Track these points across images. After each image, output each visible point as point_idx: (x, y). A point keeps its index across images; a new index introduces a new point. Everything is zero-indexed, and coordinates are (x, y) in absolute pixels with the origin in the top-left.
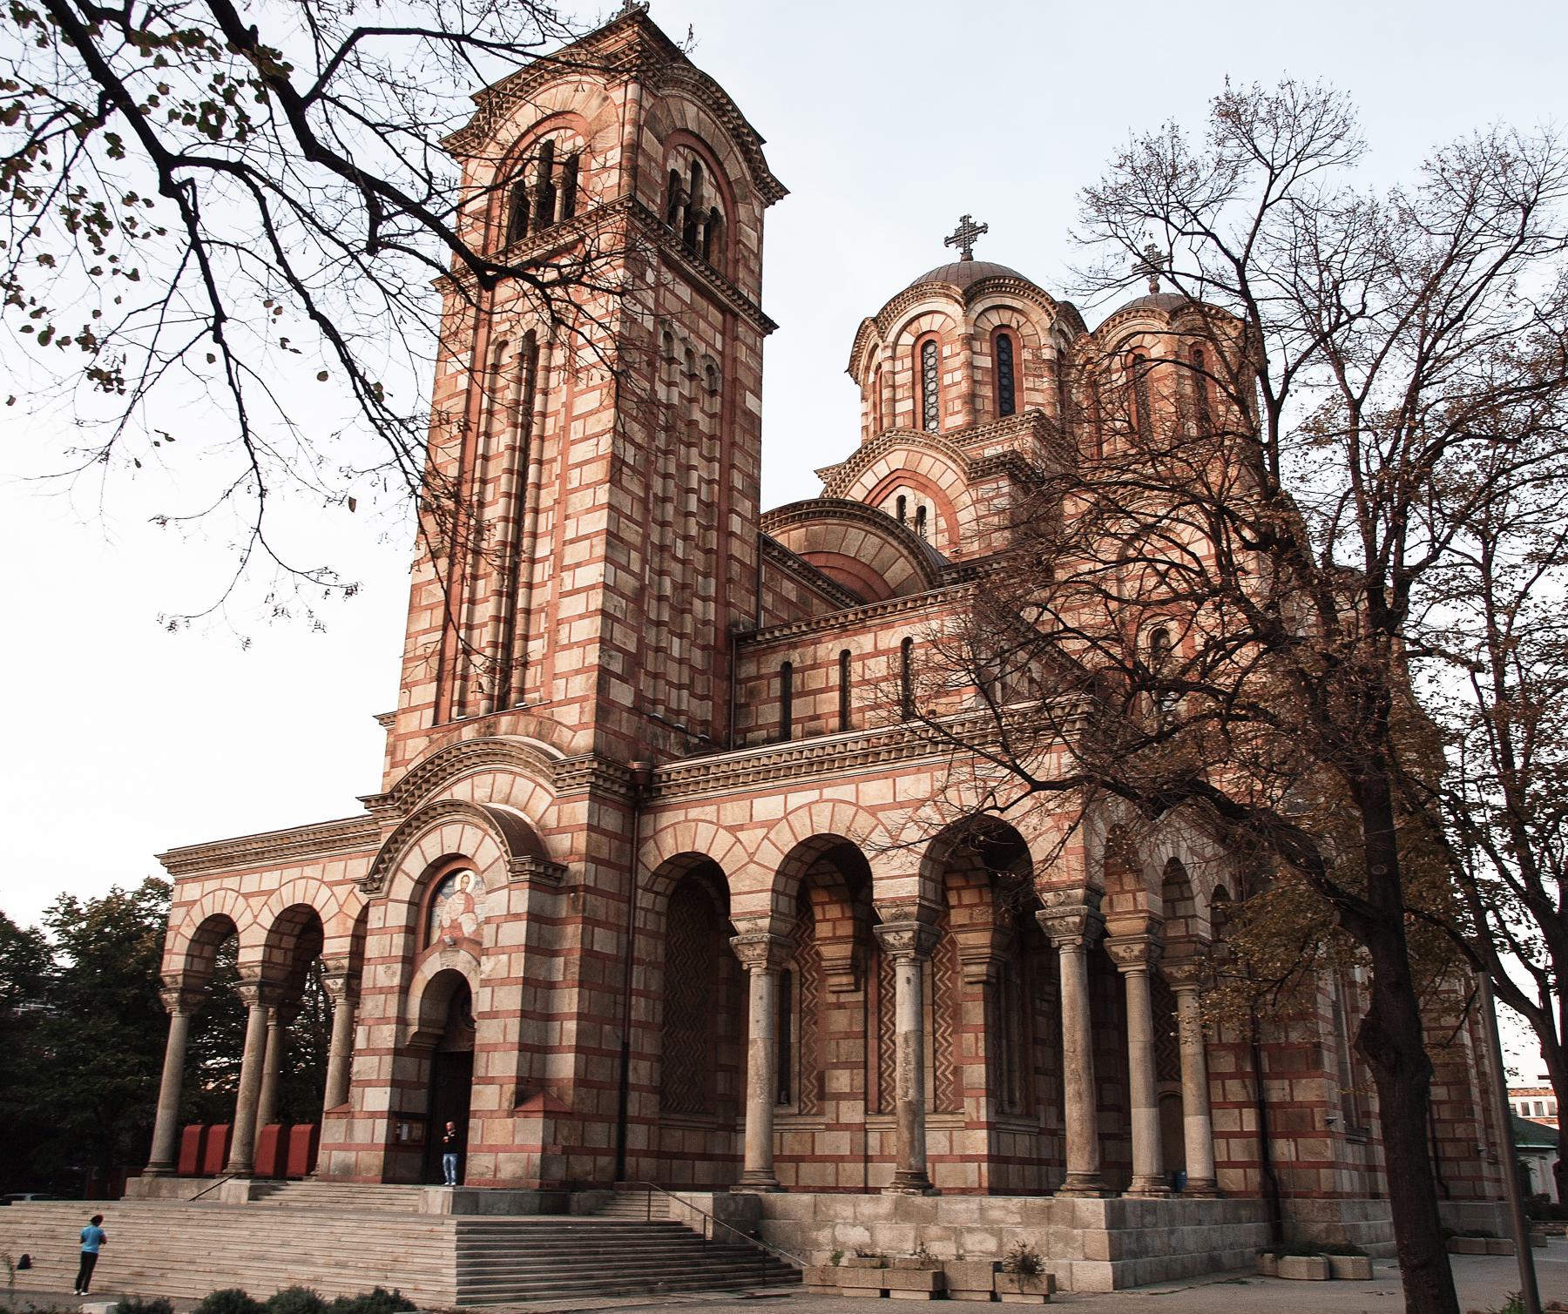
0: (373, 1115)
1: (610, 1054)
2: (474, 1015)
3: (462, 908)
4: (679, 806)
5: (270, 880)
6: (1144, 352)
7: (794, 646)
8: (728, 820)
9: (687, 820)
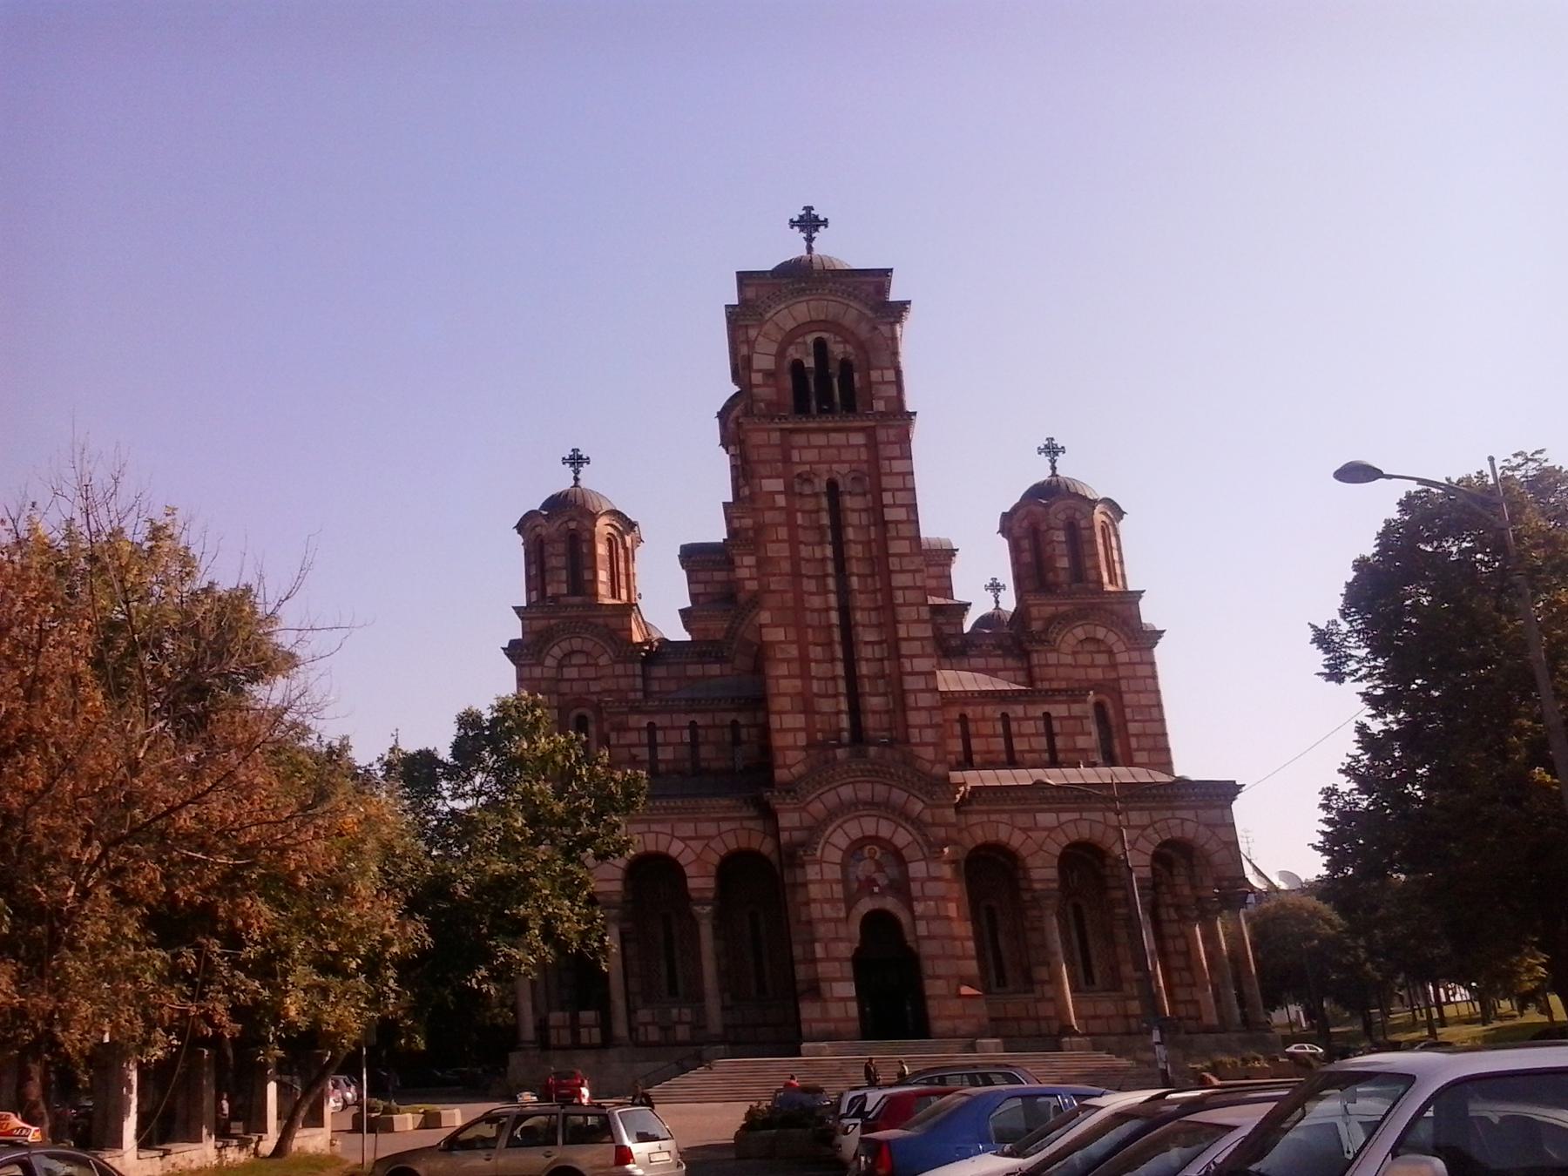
3: (873, 868)
4: (982, 812)
7: (966, 704)
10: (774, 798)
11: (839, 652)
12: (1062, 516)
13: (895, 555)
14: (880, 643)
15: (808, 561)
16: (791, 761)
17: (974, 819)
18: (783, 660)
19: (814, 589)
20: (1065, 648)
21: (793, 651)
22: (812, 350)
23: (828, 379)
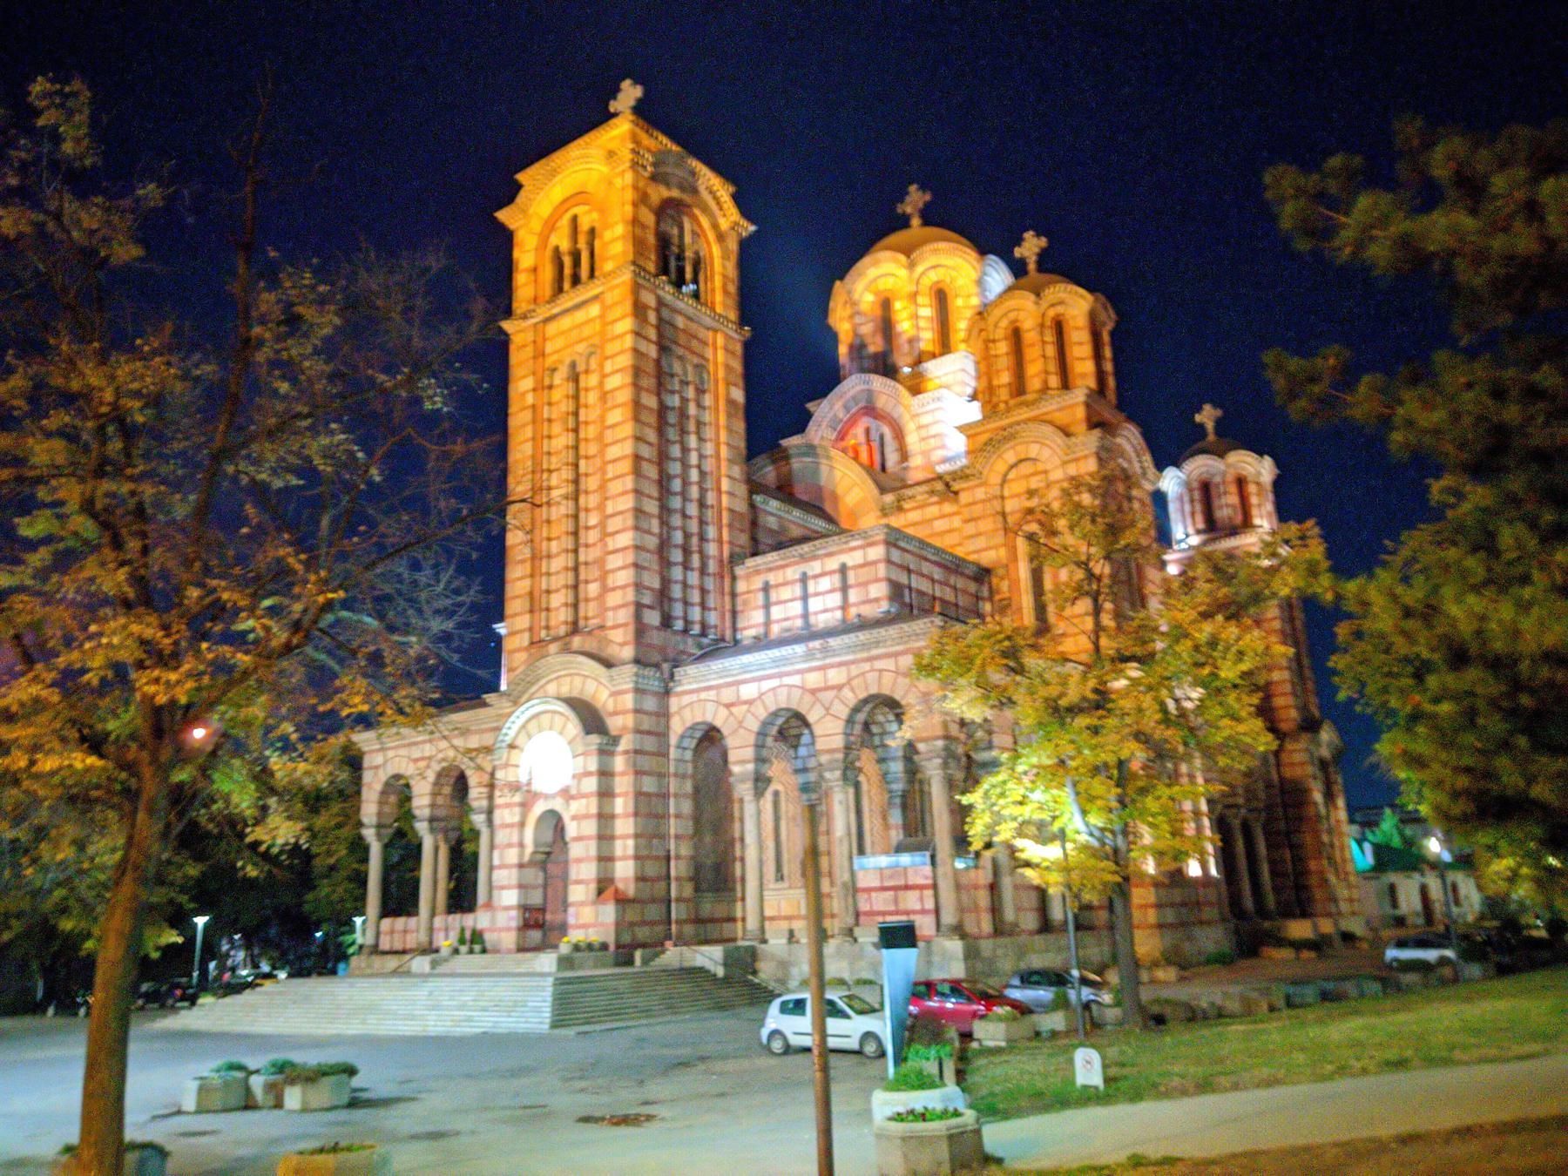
0: (507, 908)
1: (657, 858)
2: (567, 839)
8: (726, 700)
12: (1004, 323)
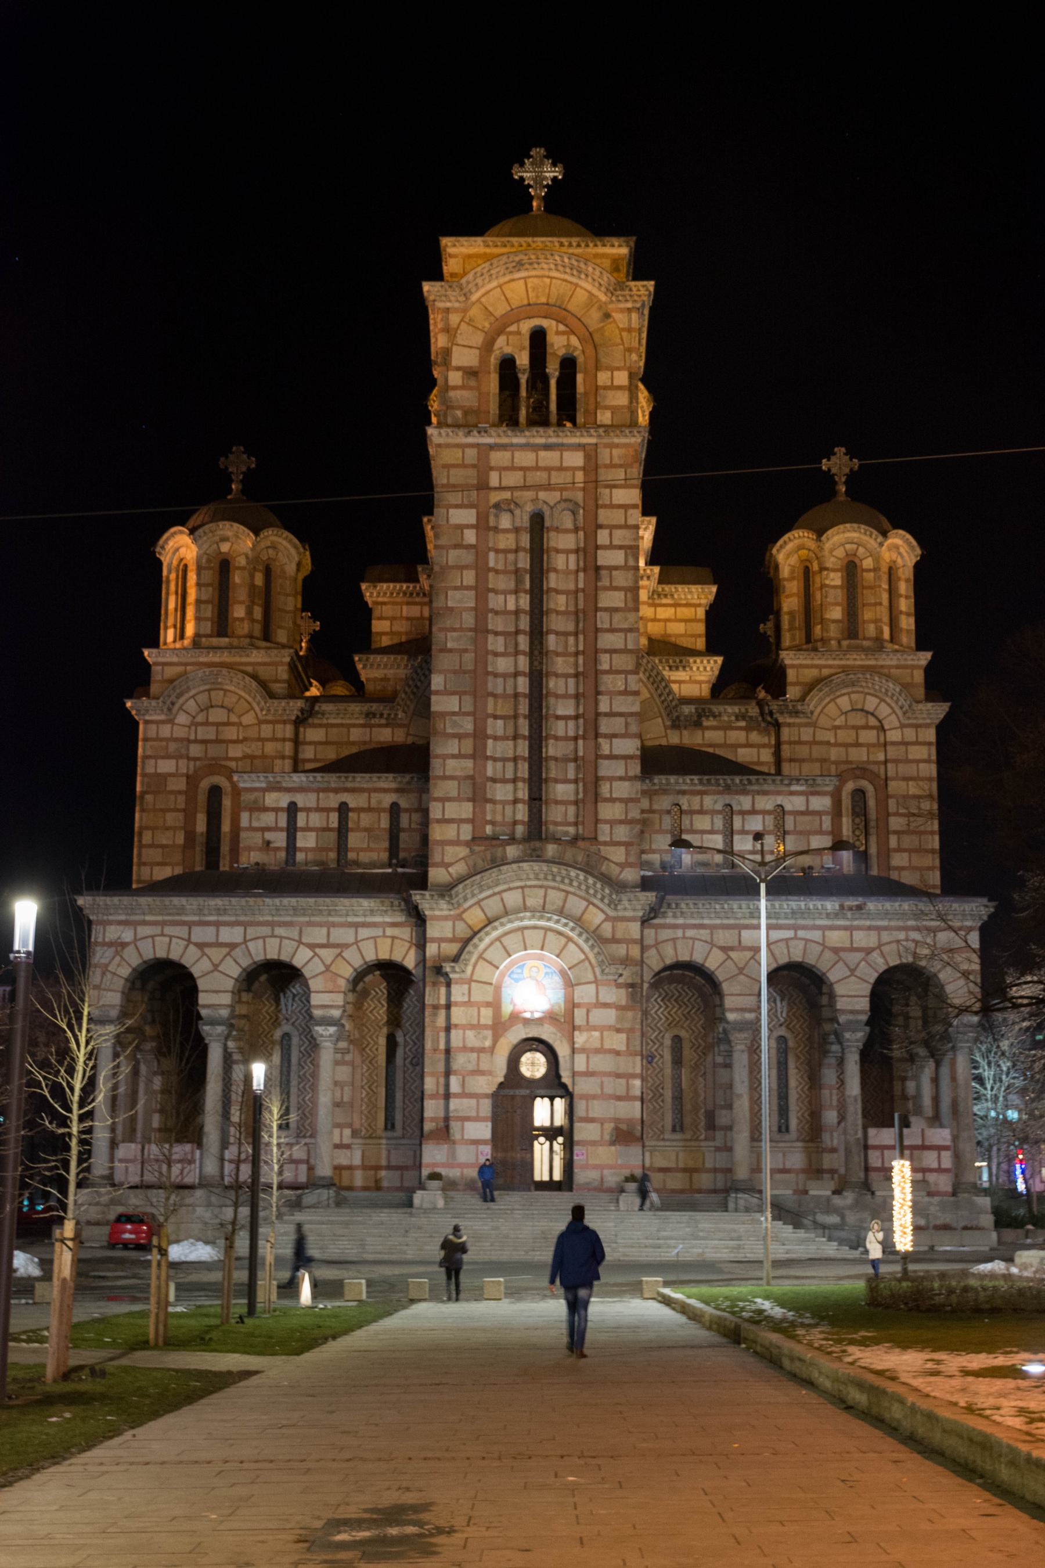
5: (229, 935)
6: (857, 561)
7: (683, 793)
8: (722, 943)
9: (684, 937)
10: (423, 900)
11: (524, 728)
12: (840, 553)
13: (606, 609)
14: (576, 717)
15: (496, 613)
16: (449, 860)
17: (665, 934)
18: (455, 736)
19: (501, 649)
20: (823, 721)
21: (468, 725)
22: (527, 343)
23: (546, 379)
